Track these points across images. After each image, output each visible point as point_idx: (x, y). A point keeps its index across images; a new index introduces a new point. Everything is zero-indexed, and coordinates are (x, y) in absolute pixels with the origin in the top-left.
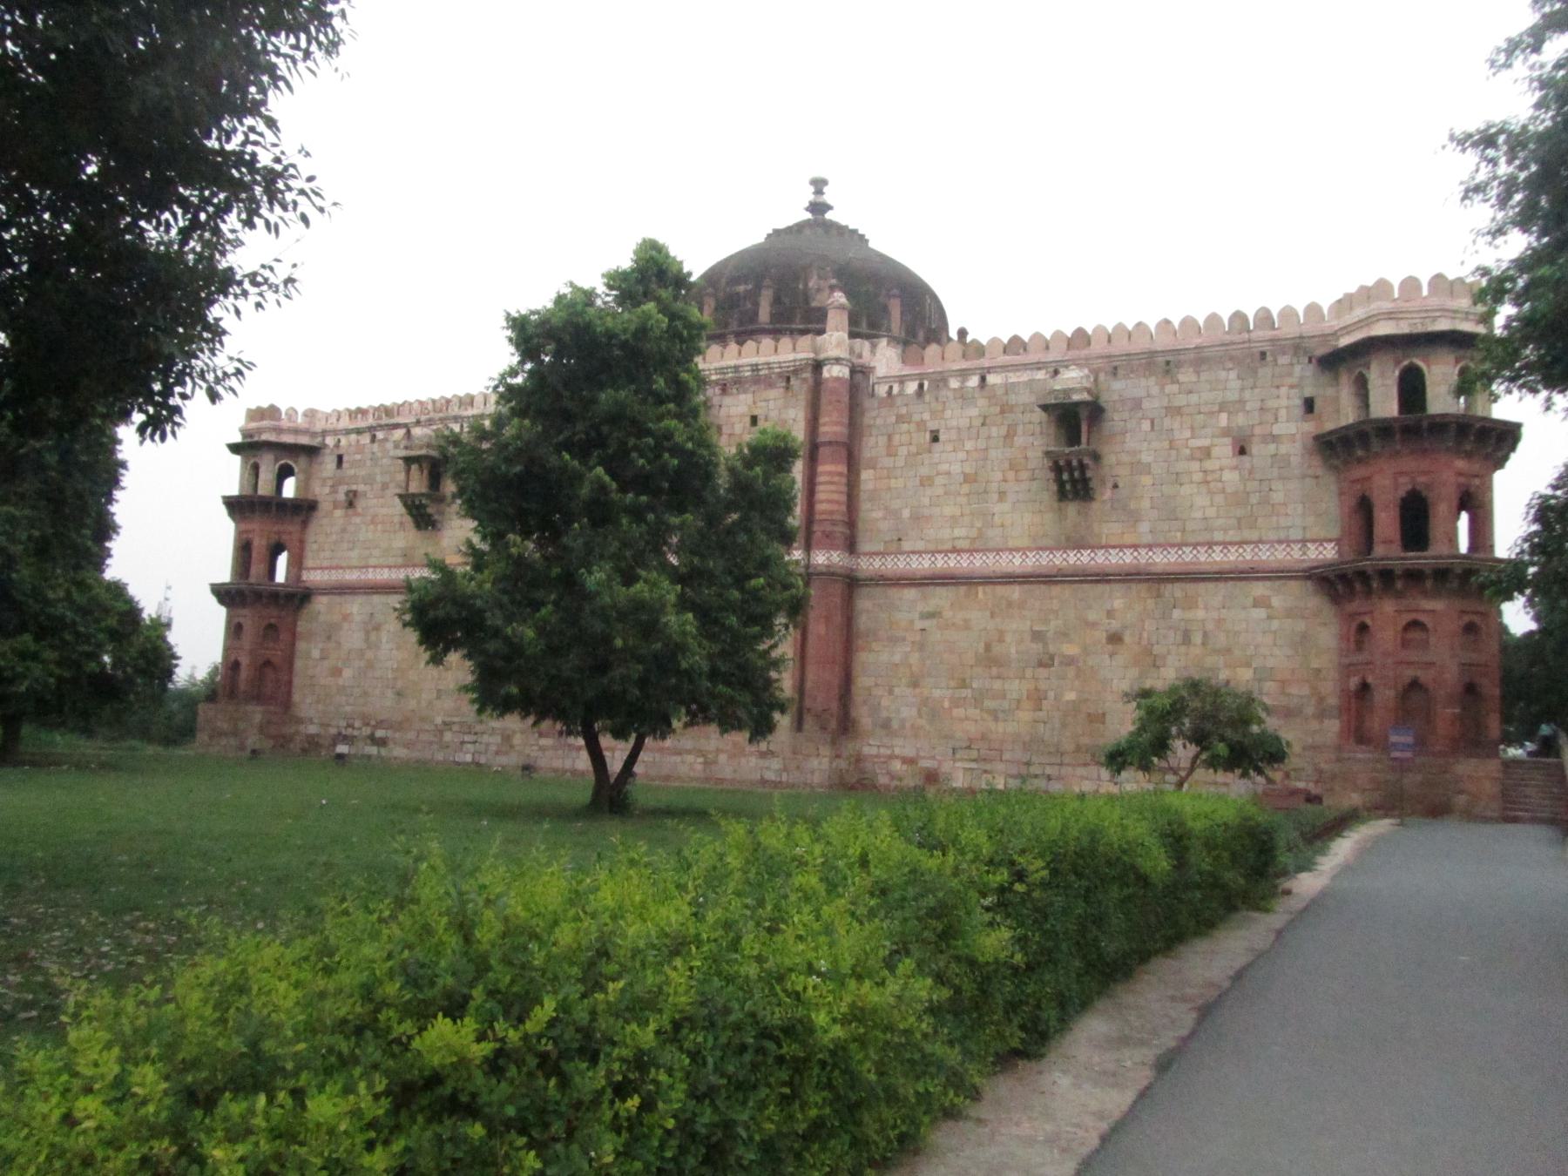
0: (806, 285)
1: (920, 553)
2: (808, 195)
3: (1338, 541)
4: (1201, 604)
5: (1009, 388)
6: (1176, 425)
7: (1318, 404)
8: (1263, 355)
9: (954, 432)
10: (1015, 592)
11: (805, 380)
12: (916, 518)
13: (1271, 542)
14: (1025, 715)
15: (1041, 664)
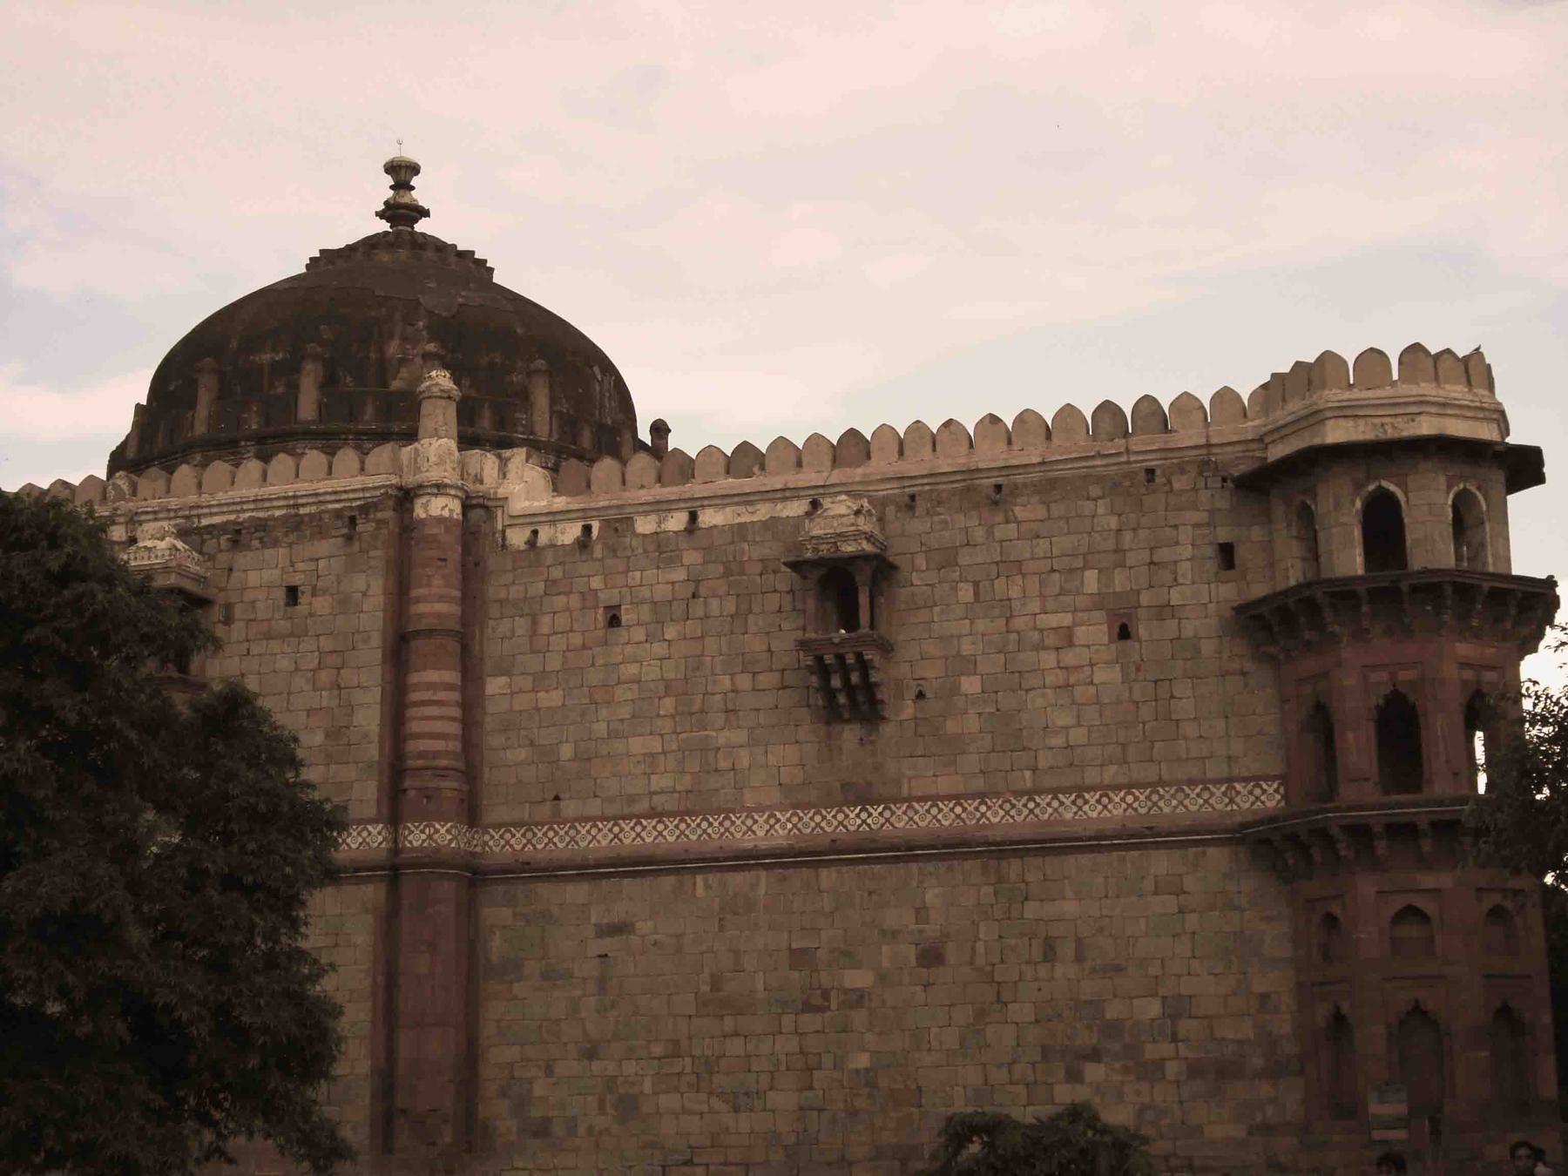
0: (382, 352)
1: (592, 819)
2: (383, 189)
3: (1283, 779)
5: (740, 531)
6: (1015, 593)
7: (1241, 554)
8: (1150, 472)
9: (645, 608)
10: (763, 883)
11: (381, 523)
12: (584, 758)
13: (1178, 783)
14: (784, 1099)
15: (808, 1007)
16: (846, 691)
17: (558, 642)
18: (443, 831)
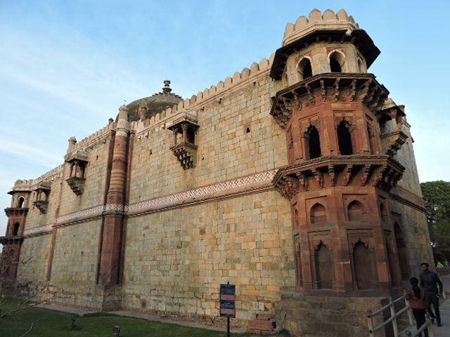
4: (234, 210)
8: (255, 83)
10: (170, 213)
12: (144, 187)
14: (172, 273)
15: (178, 247)
16: (186, 159)
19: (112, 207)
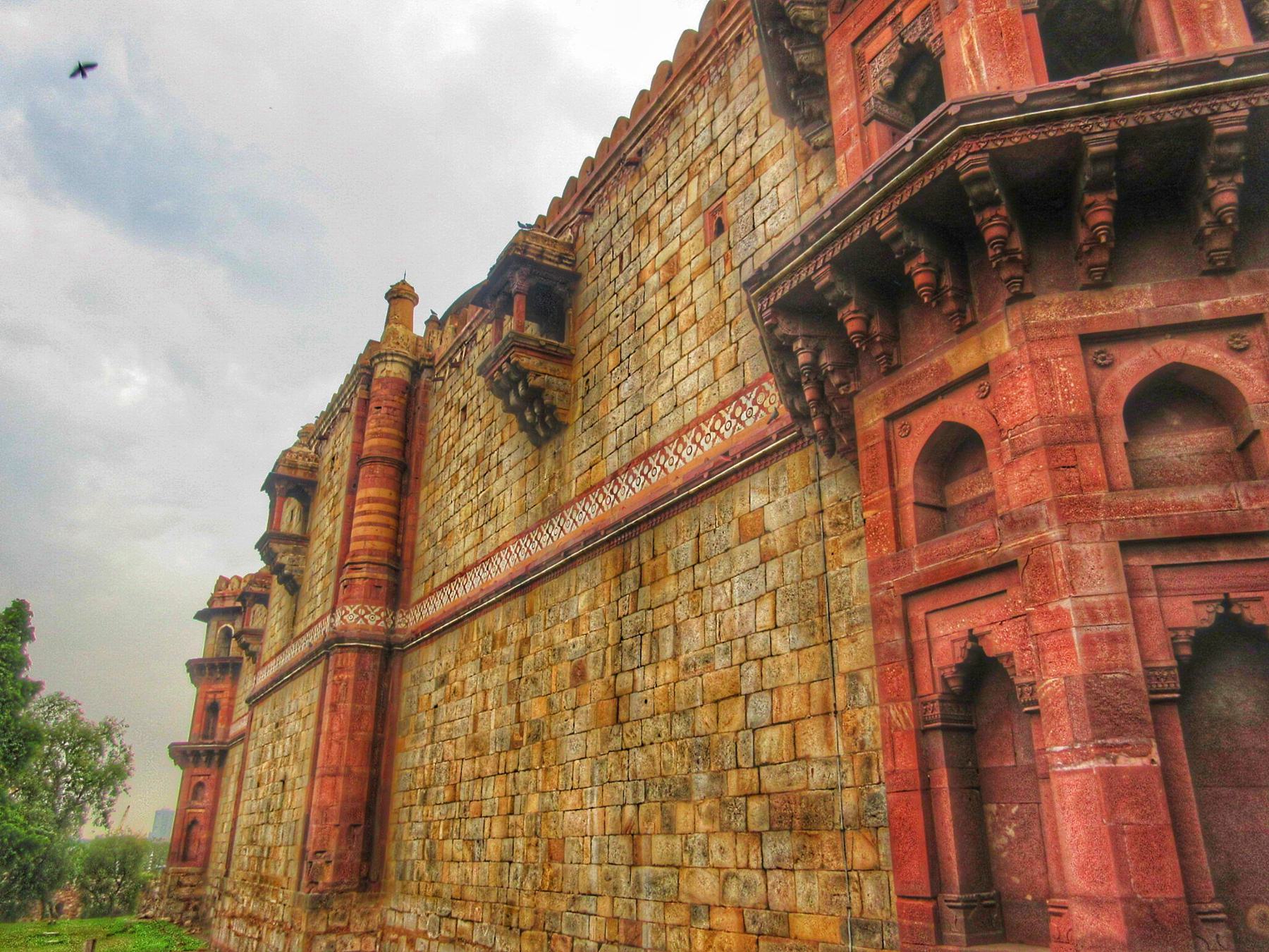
12: (444, 537)
15: (515, 746)
17: (445, 448)
18: (351, 612)
19: (357, 617)
